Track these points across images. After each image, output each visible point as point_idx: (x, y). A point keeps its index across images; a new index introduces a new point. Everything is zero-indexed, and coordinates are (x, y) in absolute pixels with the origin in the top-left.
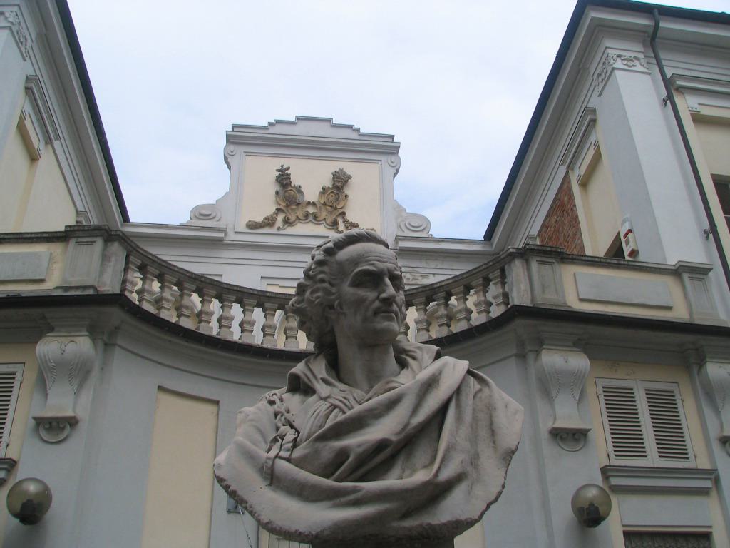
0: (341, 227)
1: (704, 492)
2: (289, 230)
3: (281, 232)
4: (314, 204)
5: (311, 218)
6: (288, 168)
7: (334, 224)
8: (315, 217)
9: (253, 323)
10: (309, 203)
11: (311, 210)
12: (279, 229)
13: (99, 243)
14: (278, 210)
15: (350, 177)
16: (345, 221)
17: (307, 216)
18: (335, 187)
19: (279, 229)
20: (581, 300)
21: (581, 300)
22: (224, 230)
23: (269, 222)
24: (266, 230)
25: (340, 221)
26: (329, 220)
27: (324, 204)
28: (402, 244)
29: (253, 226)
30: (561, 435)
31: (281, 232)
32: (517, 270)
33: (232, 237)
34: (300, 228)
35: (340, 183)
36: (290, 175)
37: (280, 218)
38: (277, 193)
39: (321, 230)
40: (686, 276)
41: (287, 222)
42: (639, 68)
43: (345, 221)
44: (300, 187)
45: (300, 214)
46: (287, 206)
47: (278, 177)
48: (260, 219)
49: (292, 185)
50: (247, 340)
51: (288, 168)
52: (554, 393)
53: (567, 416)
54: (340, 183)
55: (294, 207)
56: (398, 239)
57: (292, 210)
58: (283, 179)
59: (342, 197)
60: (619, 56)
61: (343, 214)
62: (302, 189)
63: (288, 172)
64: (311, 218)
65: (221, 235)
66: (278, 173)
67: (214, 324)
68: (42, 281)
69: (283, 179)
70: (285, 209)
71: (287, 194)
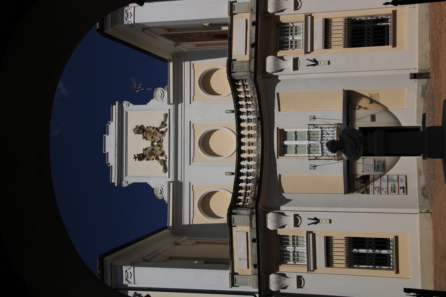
0: (164, 129)
1: (312, 18)
2: (167, 153)
3: (168, 157)
4: (152, 143)
5: (160, 144)
6: (135, 155)
7: (163, 133)
8: (160, 141)
9: (248, 165)
10: (152, 145)
11: (155, 144)
12: (166, 158)
13: (233, 216)
14: (157, 158)
15: (137, 126)
16: (160, 127)
17: (159, 146)
18: (142, 133)
19: (166, 158)
20: (246, 54)
21: (246, 54)
22: (169, 183)
23: (163, 163)
24: (167, 163)
25: (161, 130)
26: (161, 135)
27: (152, 138)
28: (172, 101)
29: (165, 170)
30: (296, 67)
31: (168, 157)
32: (236, 75)
33: (172, 179)
34: (165, 148)
35: (140, 130)
36: (138, 155)
37: (161, 158)
38: (147, 160)
39: (165, 139)
40: (234, 12)
41: (163, 154)
42: (132, 10)
43: (160, 127)
44: (143, 149)
45: (157, 149)
46: (154, 155)
47: (140, 160)
48: (162, 167)
49: (142, 153)
50: (255, 167)
51: (135, 155)
52: (281, 69)
53: (289, 64)
54: (140, 130)
55: (154, 152)
56: (169, 103)
57: (156, 152)
58: (141, 157)
59: (147, 129)
60: (126, 19)
61: (157, 128)
62: (145, 148)
63: (136, 156)
64: (160, 144)
65: (171, 184)
66: (137, 159)
67: (250, 178)
68: (247, 233)
69: (141, 157)
70: (156, 156)
71: (148, 155)
